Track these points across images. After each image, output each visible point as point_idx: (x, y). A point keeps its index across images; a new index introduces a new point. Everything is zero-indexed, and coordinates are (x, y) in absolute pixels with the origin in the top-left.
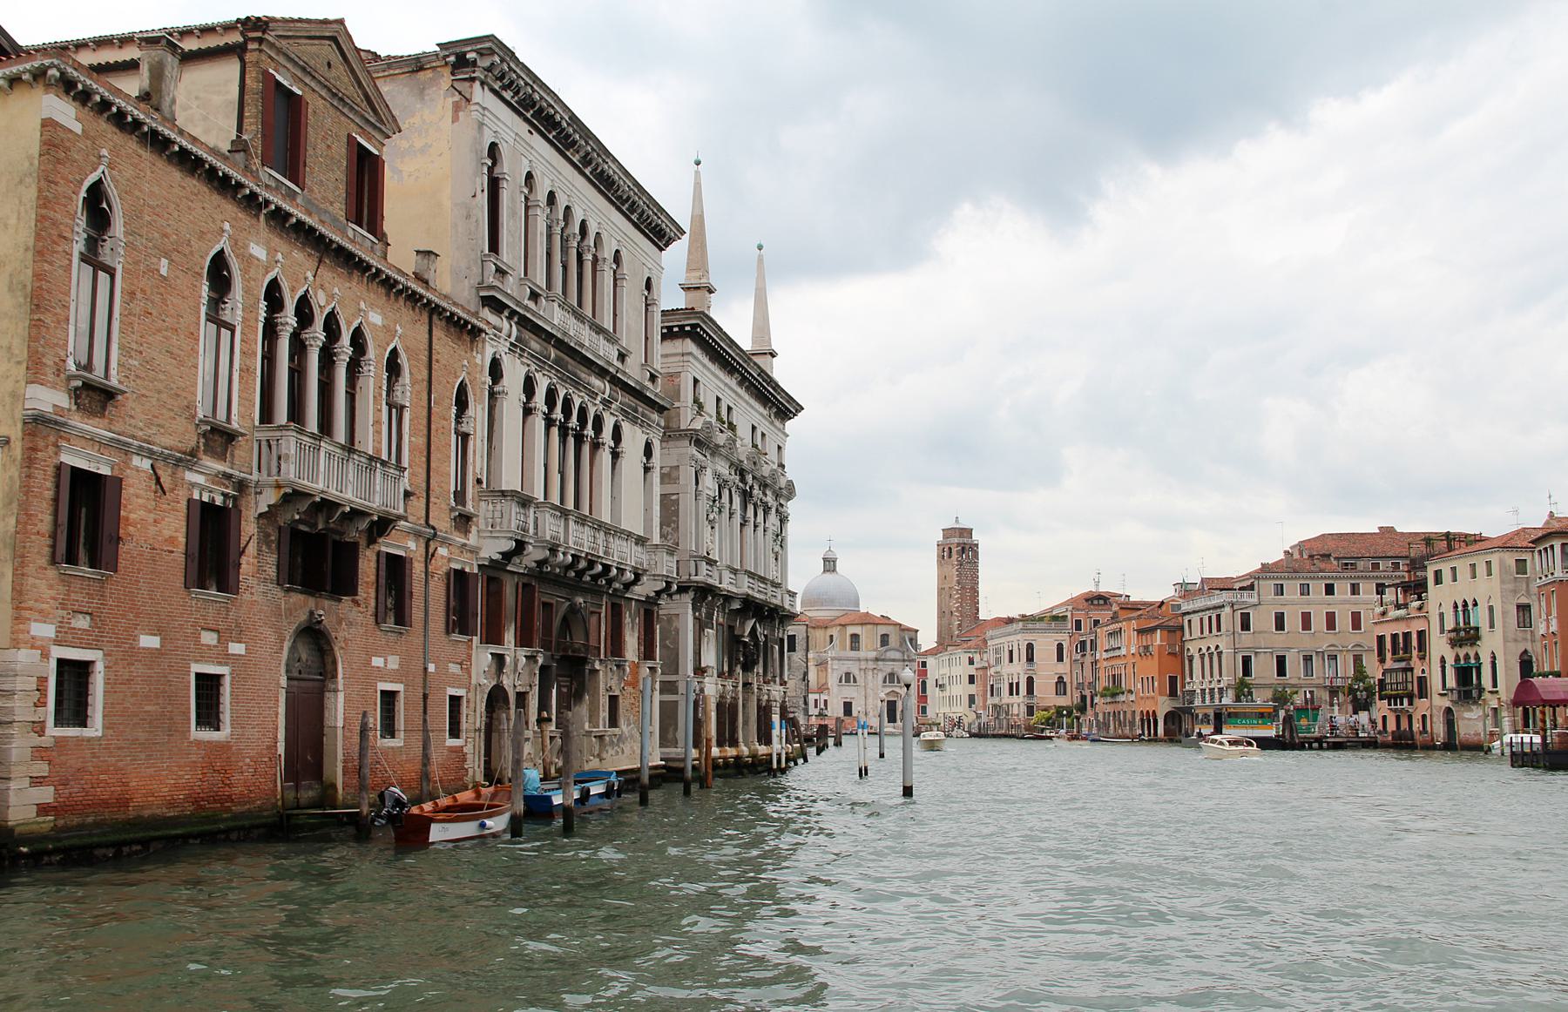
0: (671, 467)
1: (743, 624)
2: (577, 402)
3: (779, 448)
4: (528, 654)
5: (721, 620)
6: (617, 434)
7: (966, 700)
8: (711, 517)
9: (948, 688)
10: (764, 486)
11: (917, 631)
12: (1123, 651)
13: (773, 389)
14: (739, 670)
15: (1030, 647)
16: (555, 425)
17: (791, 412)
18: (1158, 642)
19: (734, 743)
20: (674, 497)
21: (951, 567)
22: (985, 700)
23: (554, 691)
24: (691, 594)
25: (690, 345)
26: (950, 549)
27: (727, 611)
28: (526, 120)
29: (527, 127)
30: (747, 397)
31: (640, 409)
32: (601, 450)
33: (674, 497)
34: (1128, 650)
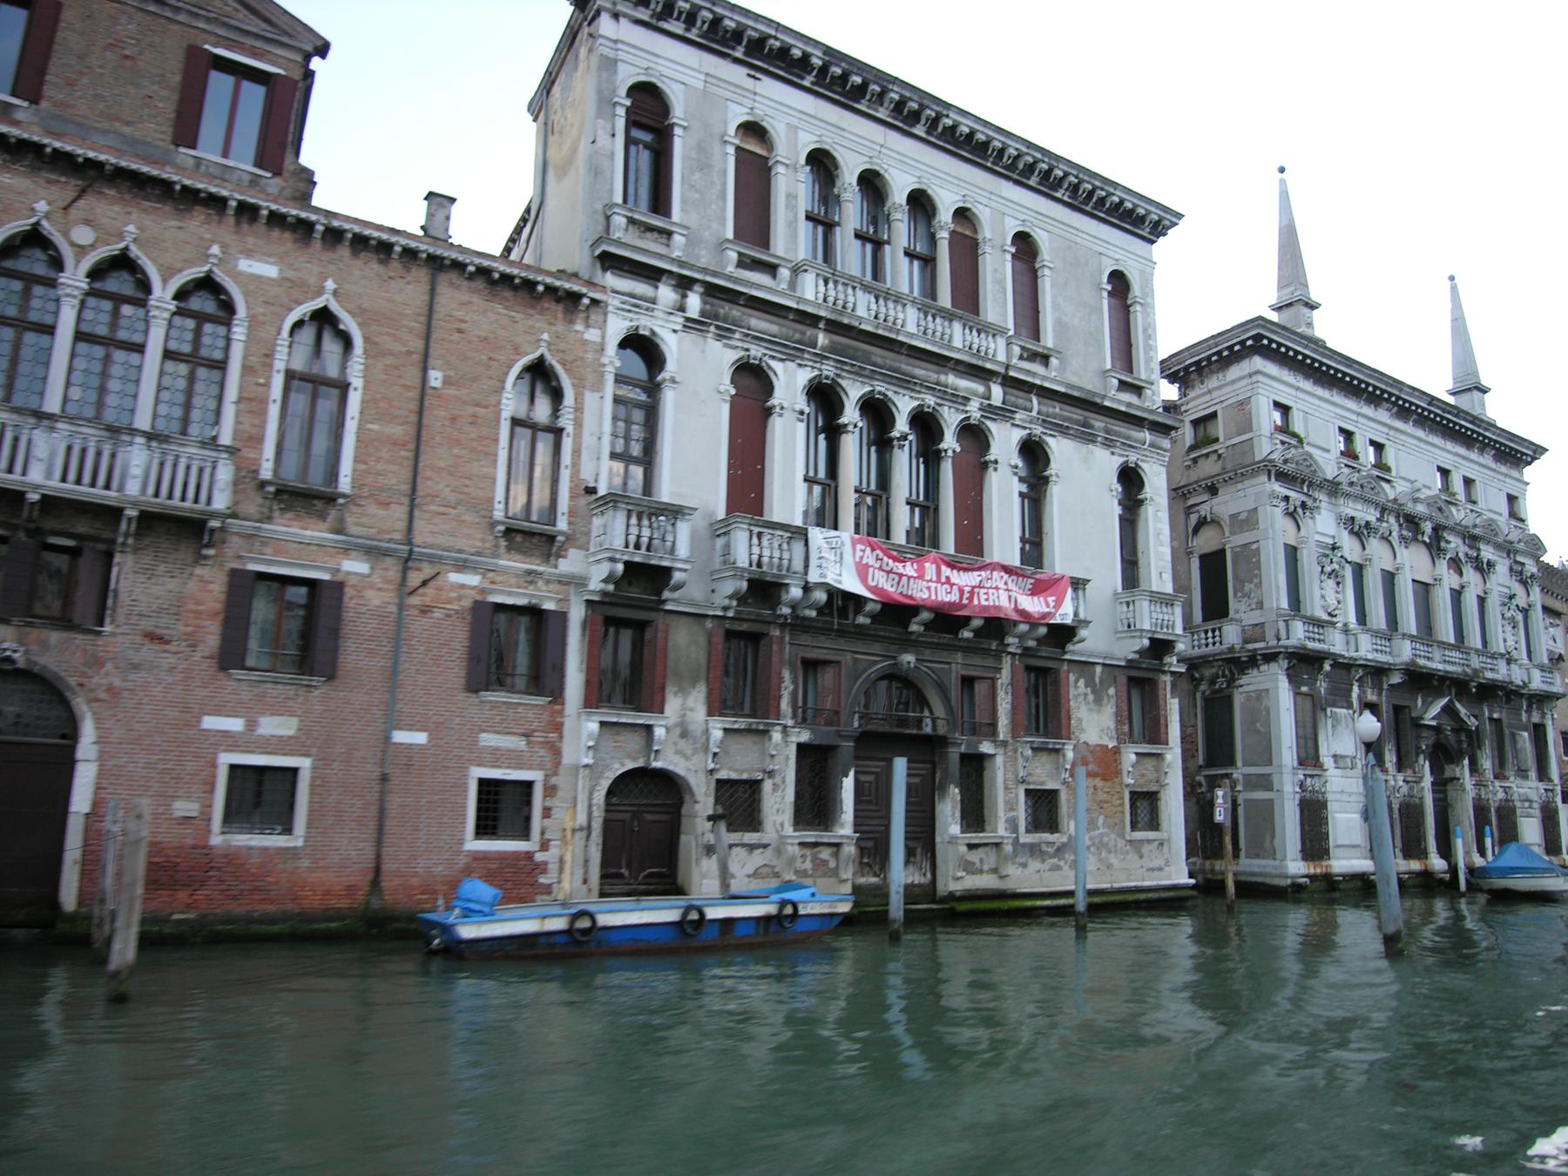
0: (1249, 511)
2: (904, 406)
3: (1512, 499)
4: (728, 726)
6: (1034, 453)
10: (1472, 539)
20: (1254, 547)
23: (848, 784)
24: (1285, 664)
25: (1258, 362)
27: (1385, 686)
28: (736, 61)
29: (744, 71)
30: (1420, 433)
31: (1098, 424)
33: (1254, 547)
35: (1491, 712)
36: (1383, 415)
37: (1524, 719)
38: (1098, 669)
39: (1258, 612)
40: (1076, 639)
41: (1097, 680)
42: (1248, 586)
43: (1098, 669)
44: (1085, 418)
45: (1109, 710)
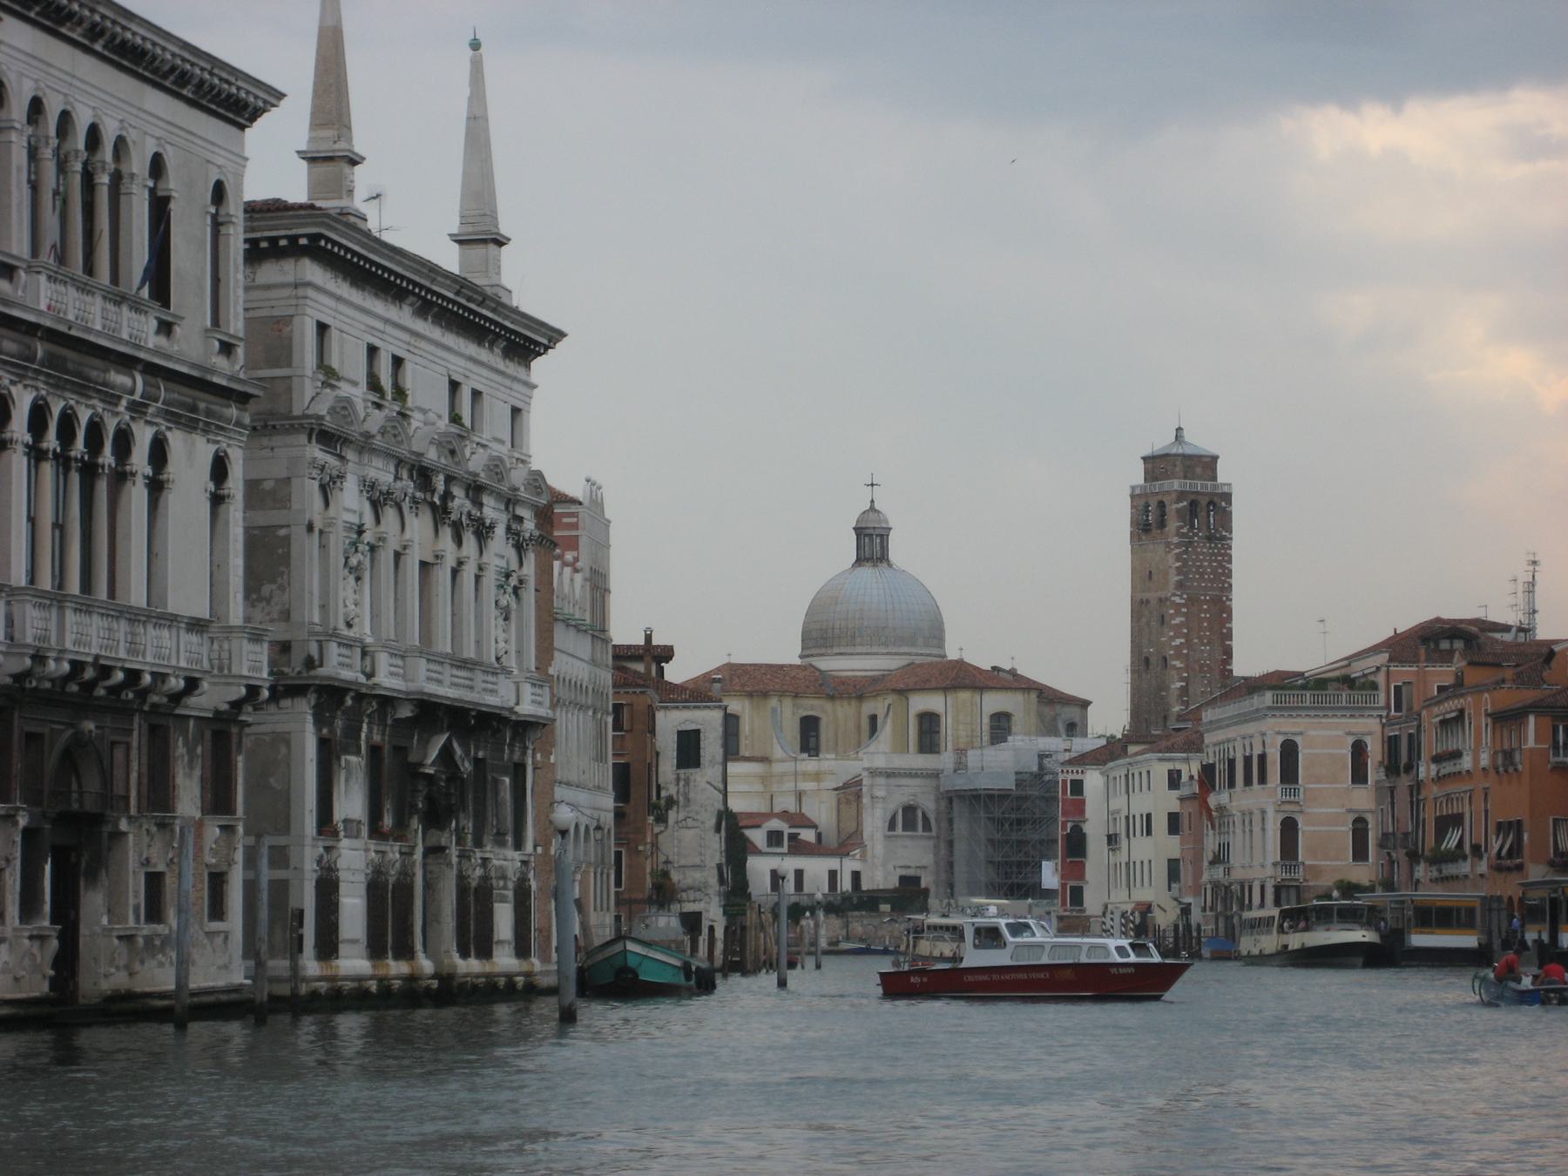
0: (277, 480)
1: (425, 743)
2: (84, 416)
3: (516, 412)
5: (377, 738)
6: (159, 453)
7: (1161, 872)
8: (354, 561)
9: (1124, 843)
10: (476, 490)
11: (1085, 704)
12: (1466, 763)
13: (494, 310)
14: (415, 823)
15: (1289, 751)
16: (47, 459)
17: (537, 344)
18: (1531, 742)
19: (404, 951)
20: (282, 532)
21: (1161, 549)
22: (1198, 874)
23: (48, 868)
24: (313, 698)
25: (312, 271)
26: (1161, 505)
27: (389, 722)
30: (436, 333)
31: (202, 405)
32: (129, 484)
33: (282, 532)
34: (1476, 760)
35: (477, 749)
36: (403, 314)
37: (506, 756)
38: (192, 723)
39: (283, 624)
40: (197, 692)
41: (190, 736)
42: (266, 589)
43: (192, 723)
44: (194, 399)
45: (197, 772)
